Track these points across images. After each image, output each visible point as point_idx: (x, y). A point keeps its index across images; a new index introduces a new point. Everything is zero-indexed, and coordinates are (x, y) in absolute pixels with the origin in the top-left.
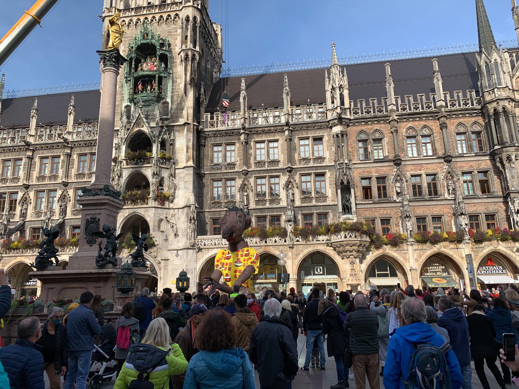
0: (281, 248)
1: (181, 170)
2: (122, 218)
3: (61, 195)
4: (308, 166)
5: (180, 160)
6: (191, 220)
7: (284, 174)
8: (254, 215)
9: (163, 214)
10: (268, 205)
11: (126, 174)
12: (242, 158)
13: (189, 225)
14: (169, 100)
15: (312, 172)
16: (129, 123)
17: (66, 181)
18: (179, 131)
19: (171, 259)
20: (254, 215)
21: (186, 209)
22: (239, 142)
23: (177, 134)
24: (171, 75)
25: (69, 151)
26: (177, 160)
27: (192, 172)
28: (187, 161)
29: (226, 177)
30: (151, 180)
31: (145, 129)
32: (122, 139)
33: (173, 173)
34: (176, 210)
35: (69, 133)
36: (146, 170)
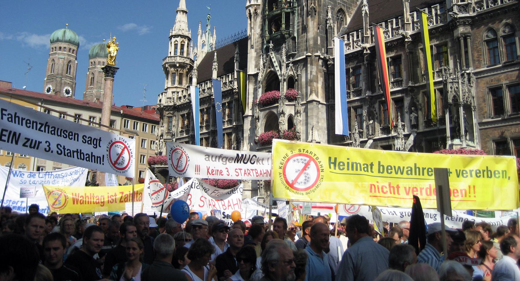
7: (407, 95)
14: (296, 35)
22: (364, 65)
24: (297, 9)
25: (237, 97)
28: (311, 94)
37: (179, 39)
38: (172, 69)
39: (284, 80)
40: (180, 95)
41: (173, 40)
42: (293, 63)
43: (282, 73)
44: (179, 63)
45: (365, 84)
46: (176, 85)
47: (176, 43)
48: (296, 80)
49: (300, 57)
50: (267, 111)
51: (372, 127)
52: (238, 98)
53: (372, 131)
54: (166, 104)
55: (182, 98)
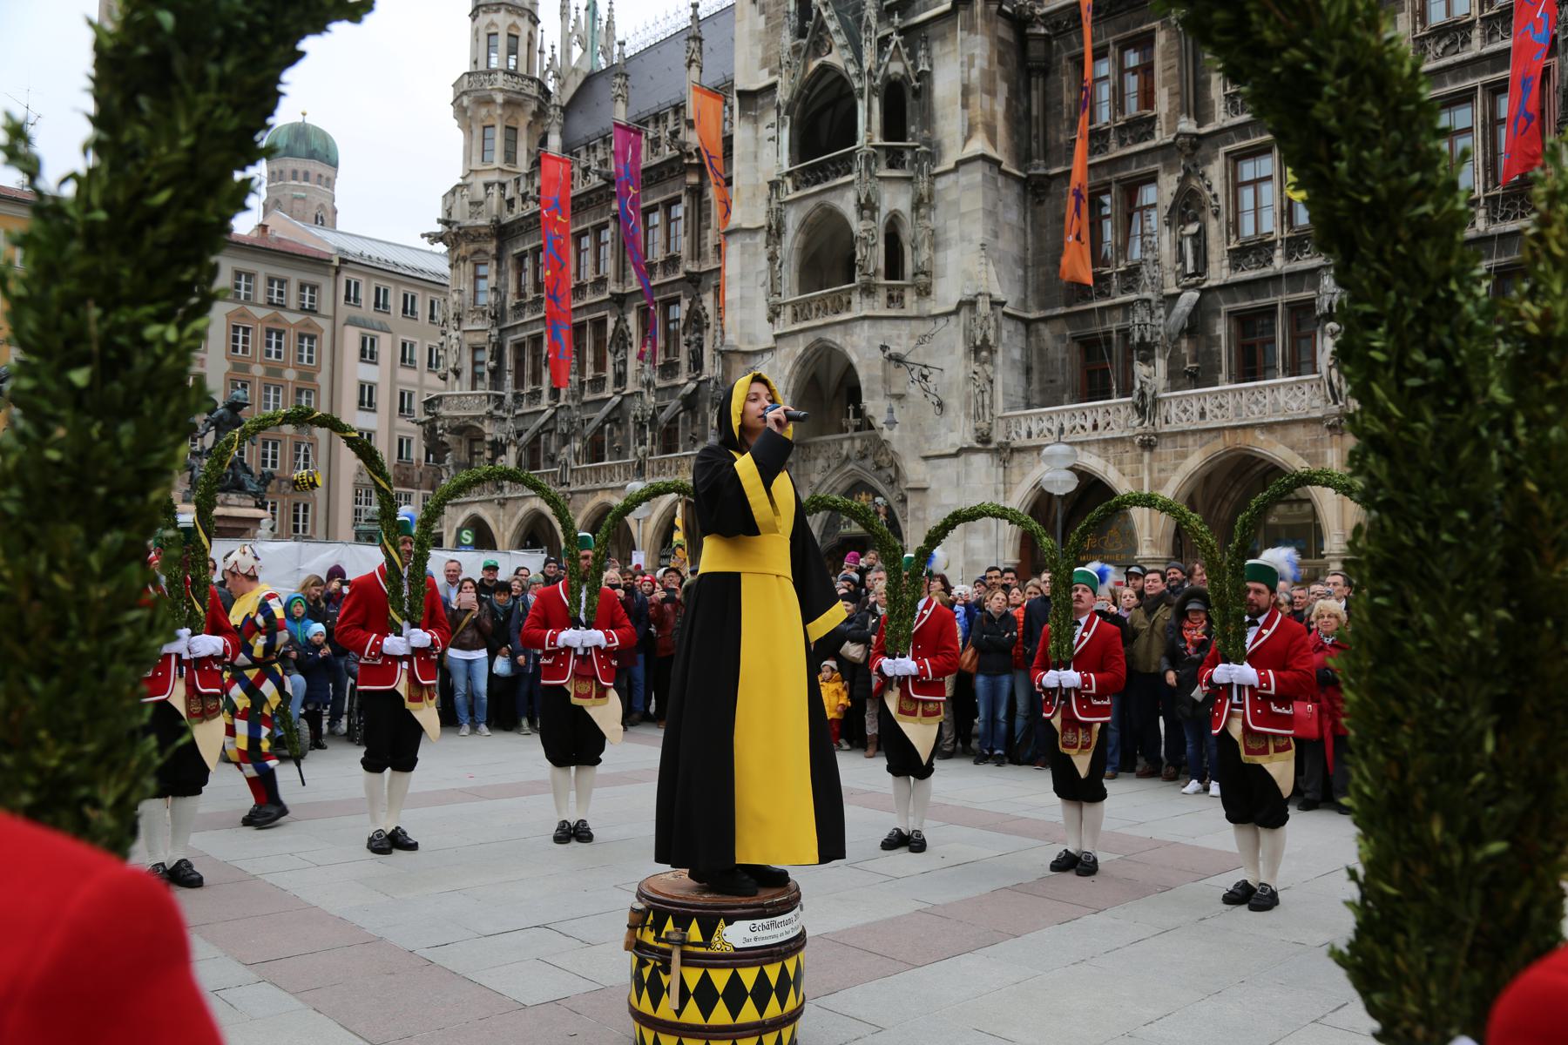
0: (1298, 433)
1: (952, 177)
2: (791, 363)
3: (688, 312)
4: (1458, 58)
5: (947, 142)
6: (977, 350)
8: (1224, 308)
9: (901, 339)
10: (1279, 263)
11: (793, 219)
12: (1176, 86)
13: (975, 367)
15: (1477, 81)
16: (796, 50)
17: (695, 270)
18: (942, 38)
19: (934, 486)
20: (1224, 308)
21: (964, 312)
23: (937, 48)
25: (693, 179)
26: (939, 145)
27: (978, 177)
28: (967, 139)
29: (1124, 174)
30: (857, 227)
31: (837, 58)
32: (778, 108)
33: (925, 192)
34: (942, 322)
35: (690, 124)
36: (842, 198)
37: (502, 20)
38: (483, 111)
39: (873, 90)
40: (509, 193)
41: (484, 19)
42: (901, 32)
43: (866, 66)
44: (501, 90)
45: (1171, 95)
46: (498, 160)
47: (493, 30)
48: (917, 93)
49: (926, 10)
50: (811, 203)
51: (1196, 248)
52: (701, 184)
53: (1196, 259)
54: (468, 222)
55: (518, 203)
